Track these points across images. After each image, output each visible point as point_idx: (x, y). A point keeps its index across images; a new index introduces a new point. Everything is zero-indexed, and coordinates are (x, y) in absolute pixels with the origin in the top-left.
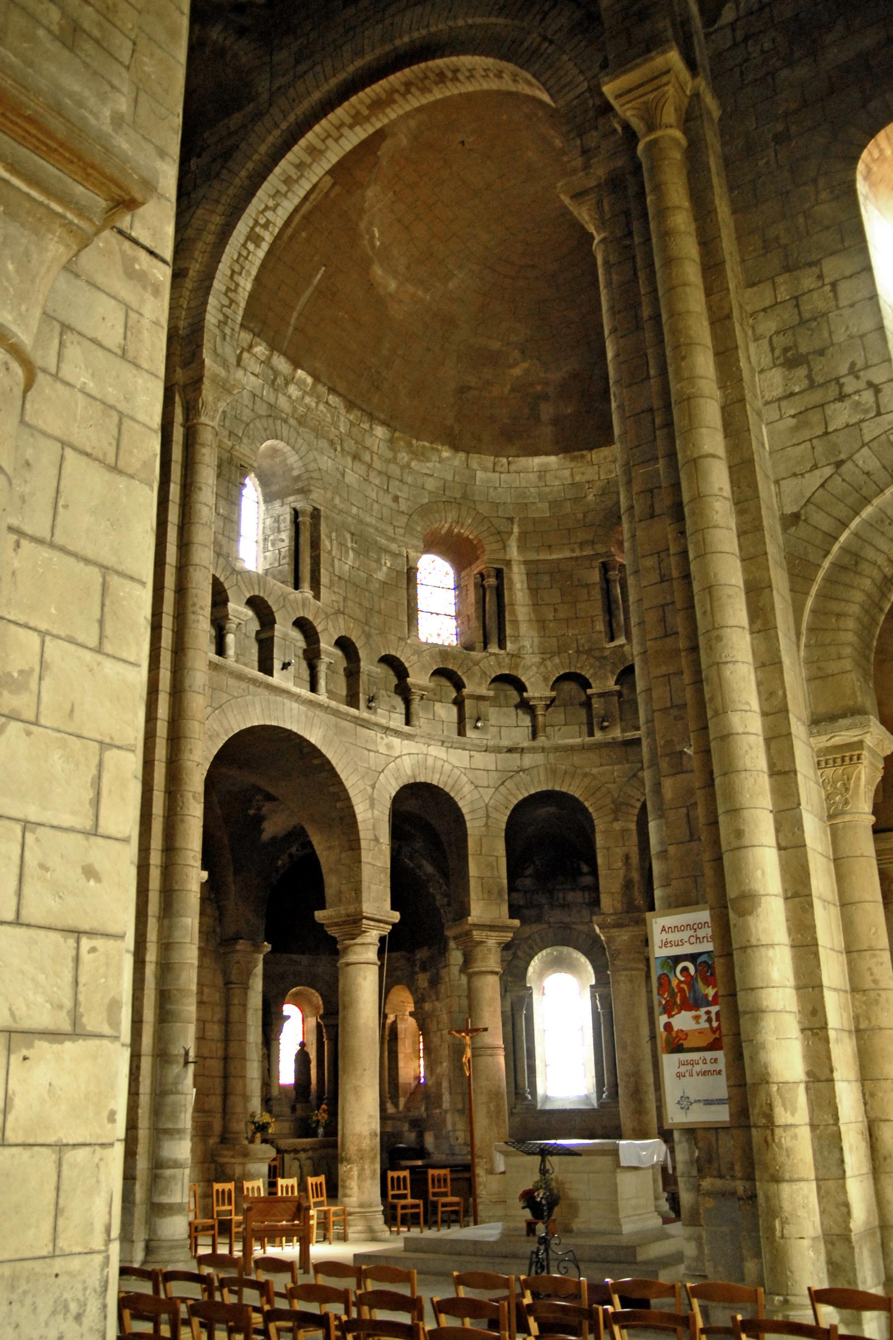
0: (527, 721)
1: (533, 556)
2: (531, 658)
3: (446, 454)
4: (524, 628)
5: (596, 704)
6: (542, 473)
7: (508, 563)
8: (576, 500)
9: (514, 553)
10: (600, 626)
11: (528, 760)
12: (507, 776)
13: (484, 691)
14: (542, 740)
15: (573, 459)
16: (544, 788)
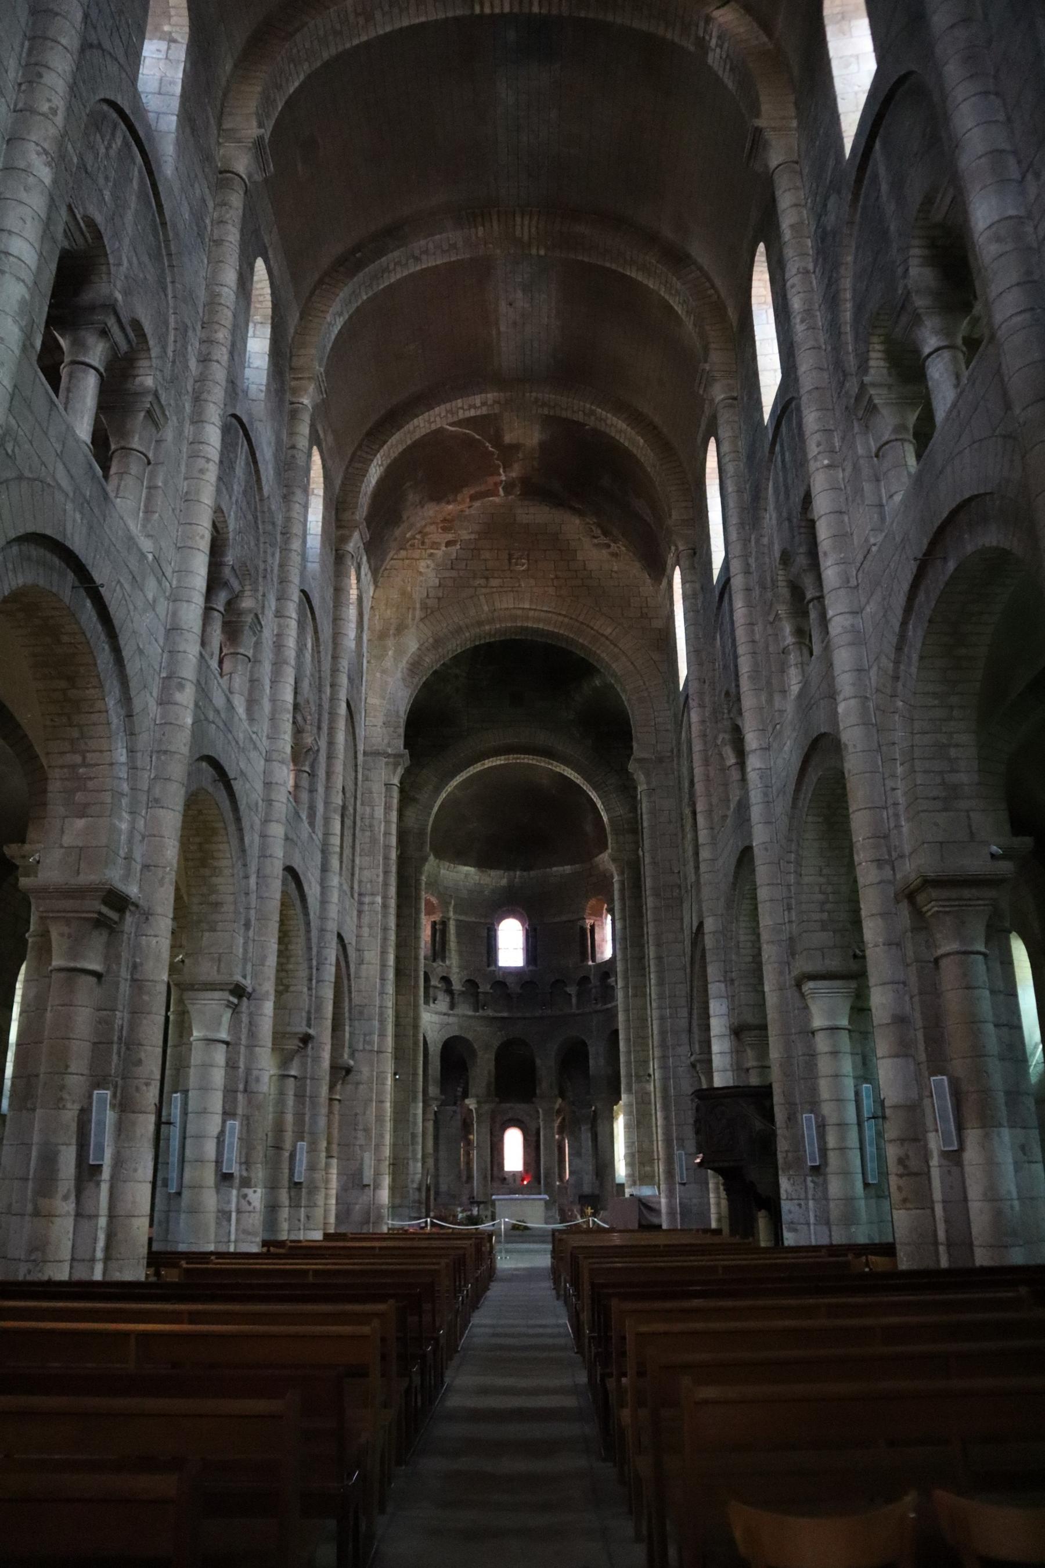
0: (448, 999)
5: (481, 997)
6: (467, 875)
7: (449, 919)
9: (451, 914)
10: (485, 959)
11: (451, 1020)
12: (444, 1026)
16: (457, 1034)
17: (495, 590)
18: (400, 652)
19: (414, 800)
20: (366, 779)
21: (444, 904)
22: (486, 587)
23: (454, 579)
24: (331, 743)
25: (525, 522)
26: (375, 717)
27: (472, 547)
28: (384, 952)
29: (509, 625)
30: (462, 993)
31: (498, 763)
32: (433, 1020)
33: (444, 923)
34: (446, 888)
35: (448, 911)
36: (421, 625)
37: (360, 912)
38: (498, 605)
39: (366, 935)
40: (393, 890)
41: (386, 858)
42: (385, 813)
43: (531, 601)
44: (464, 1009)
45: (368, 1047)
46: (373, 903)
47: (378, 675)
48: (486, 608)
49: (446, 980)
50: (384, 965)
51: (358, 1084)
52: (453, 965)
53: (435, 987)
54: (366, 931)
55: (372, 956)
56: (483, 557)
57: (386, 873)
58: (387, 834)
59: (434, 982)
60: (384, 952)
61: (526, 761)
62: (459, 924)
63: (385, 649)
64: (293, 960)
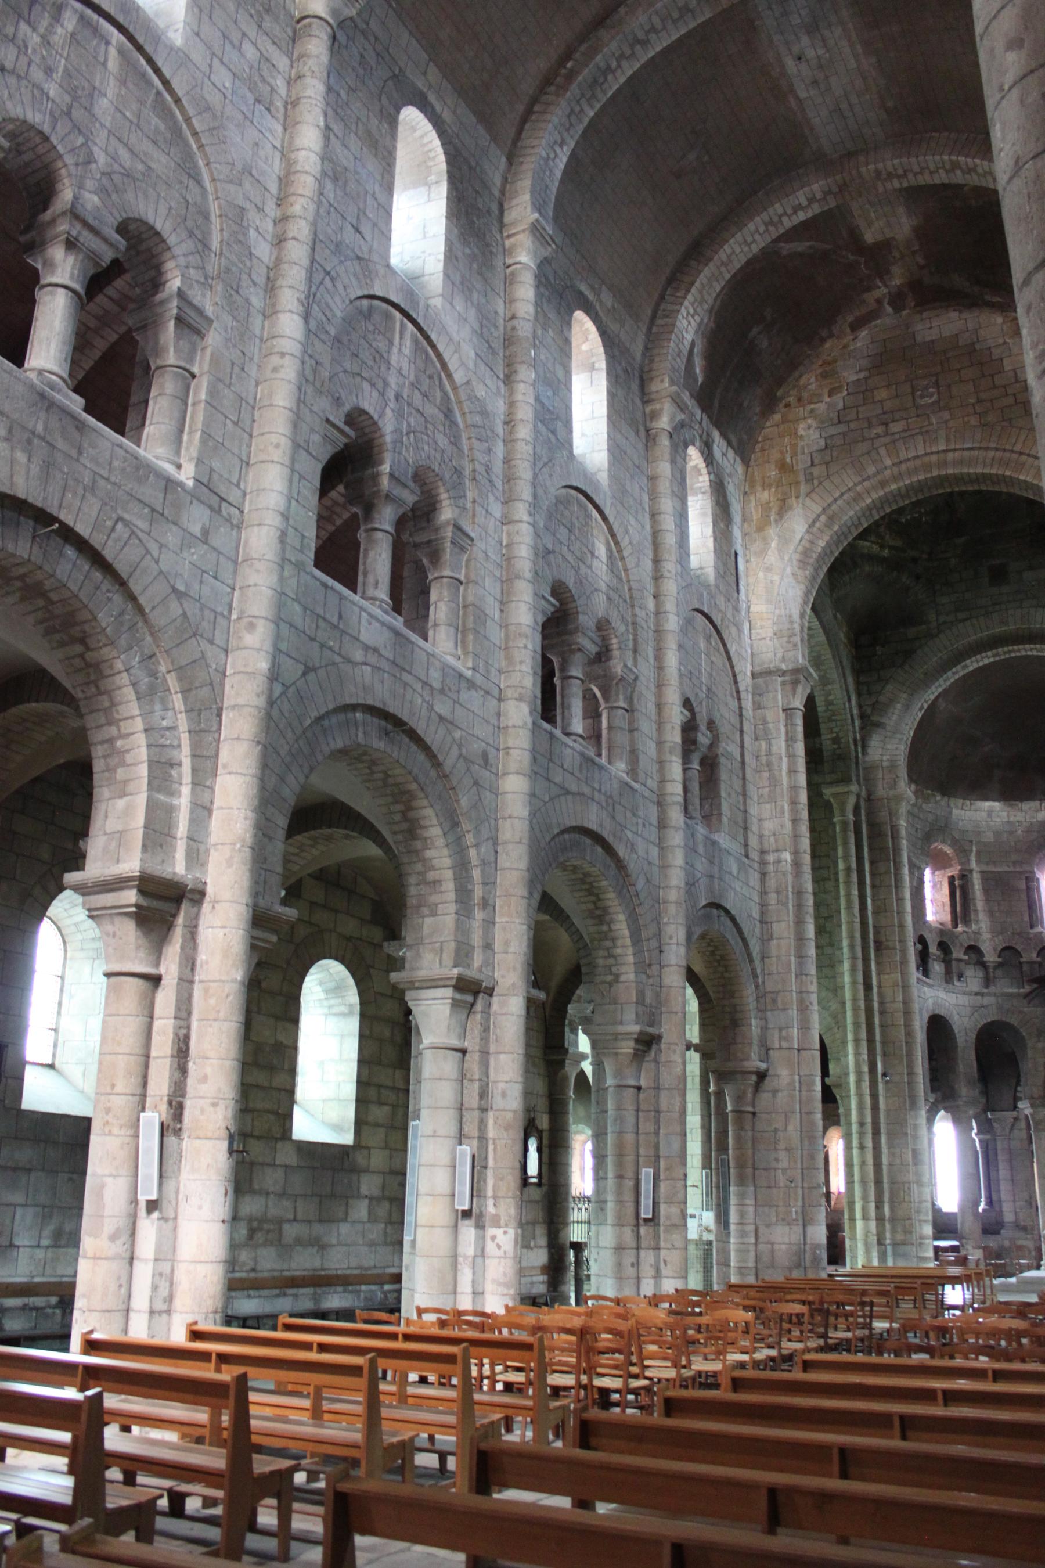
0: (981, 974)
1: (985, 868)
2: (986, 936)
3: (938, 798)
4: (982, 916)
5: (1025, 968)
6: (990, 813)
7: (971, 871)
8: (1011, 833)
9: (973, 865)
10: (1026, 918)
11: (986, 1001)
12: (976, 1009)
13: (962, 956)
14: (992, 989)
15: (1011, 806)
16: (995, 1018)
17: (897, 436)
18: (784, 541)
19: (878, 725)
20: (757, 706)
21: (962, 851)
22: (887, 434)
23: (844, 434)
24: (660, 668)
25: (928, 339)
26: (762, 627)
27: (863, 388)
28: (799, 922)
29: (922, 477)
30: (1000, 965)
31: (986, 661)
32: (961, 1002)
33: (965, 876)
34: (963, 832)
35: (969, 860)
36: (808, 501)
37: (763, 875)
38: (903, 455)
39: (773, 902)
40: (806, 843)
41: (793, 802)
42: (788, 746)
43: (948, 440)
44: (1005, 987)
45: (784, 1044)
46: (779, 861)
47: (761, 575)
48: (888, 462)
49: (973, 949)
50: (800, 939)
51: (775, 1092)
52: (983, 930)
53: (959, 960)
54: (772, 898)
55: (783, 928)
56: (877, 398)
57: (795, 821)
58: (792, 771)
59: (957, 953)
60: (799, 922)
61: (1023, 653)
62: (985, 876)
63: (766, 542)
64: (619, 943)
